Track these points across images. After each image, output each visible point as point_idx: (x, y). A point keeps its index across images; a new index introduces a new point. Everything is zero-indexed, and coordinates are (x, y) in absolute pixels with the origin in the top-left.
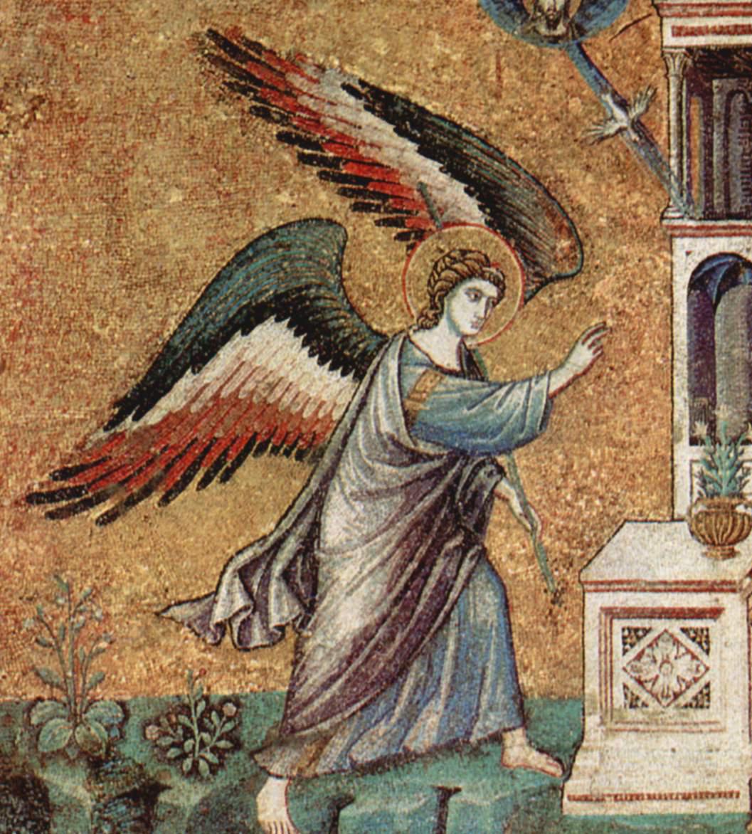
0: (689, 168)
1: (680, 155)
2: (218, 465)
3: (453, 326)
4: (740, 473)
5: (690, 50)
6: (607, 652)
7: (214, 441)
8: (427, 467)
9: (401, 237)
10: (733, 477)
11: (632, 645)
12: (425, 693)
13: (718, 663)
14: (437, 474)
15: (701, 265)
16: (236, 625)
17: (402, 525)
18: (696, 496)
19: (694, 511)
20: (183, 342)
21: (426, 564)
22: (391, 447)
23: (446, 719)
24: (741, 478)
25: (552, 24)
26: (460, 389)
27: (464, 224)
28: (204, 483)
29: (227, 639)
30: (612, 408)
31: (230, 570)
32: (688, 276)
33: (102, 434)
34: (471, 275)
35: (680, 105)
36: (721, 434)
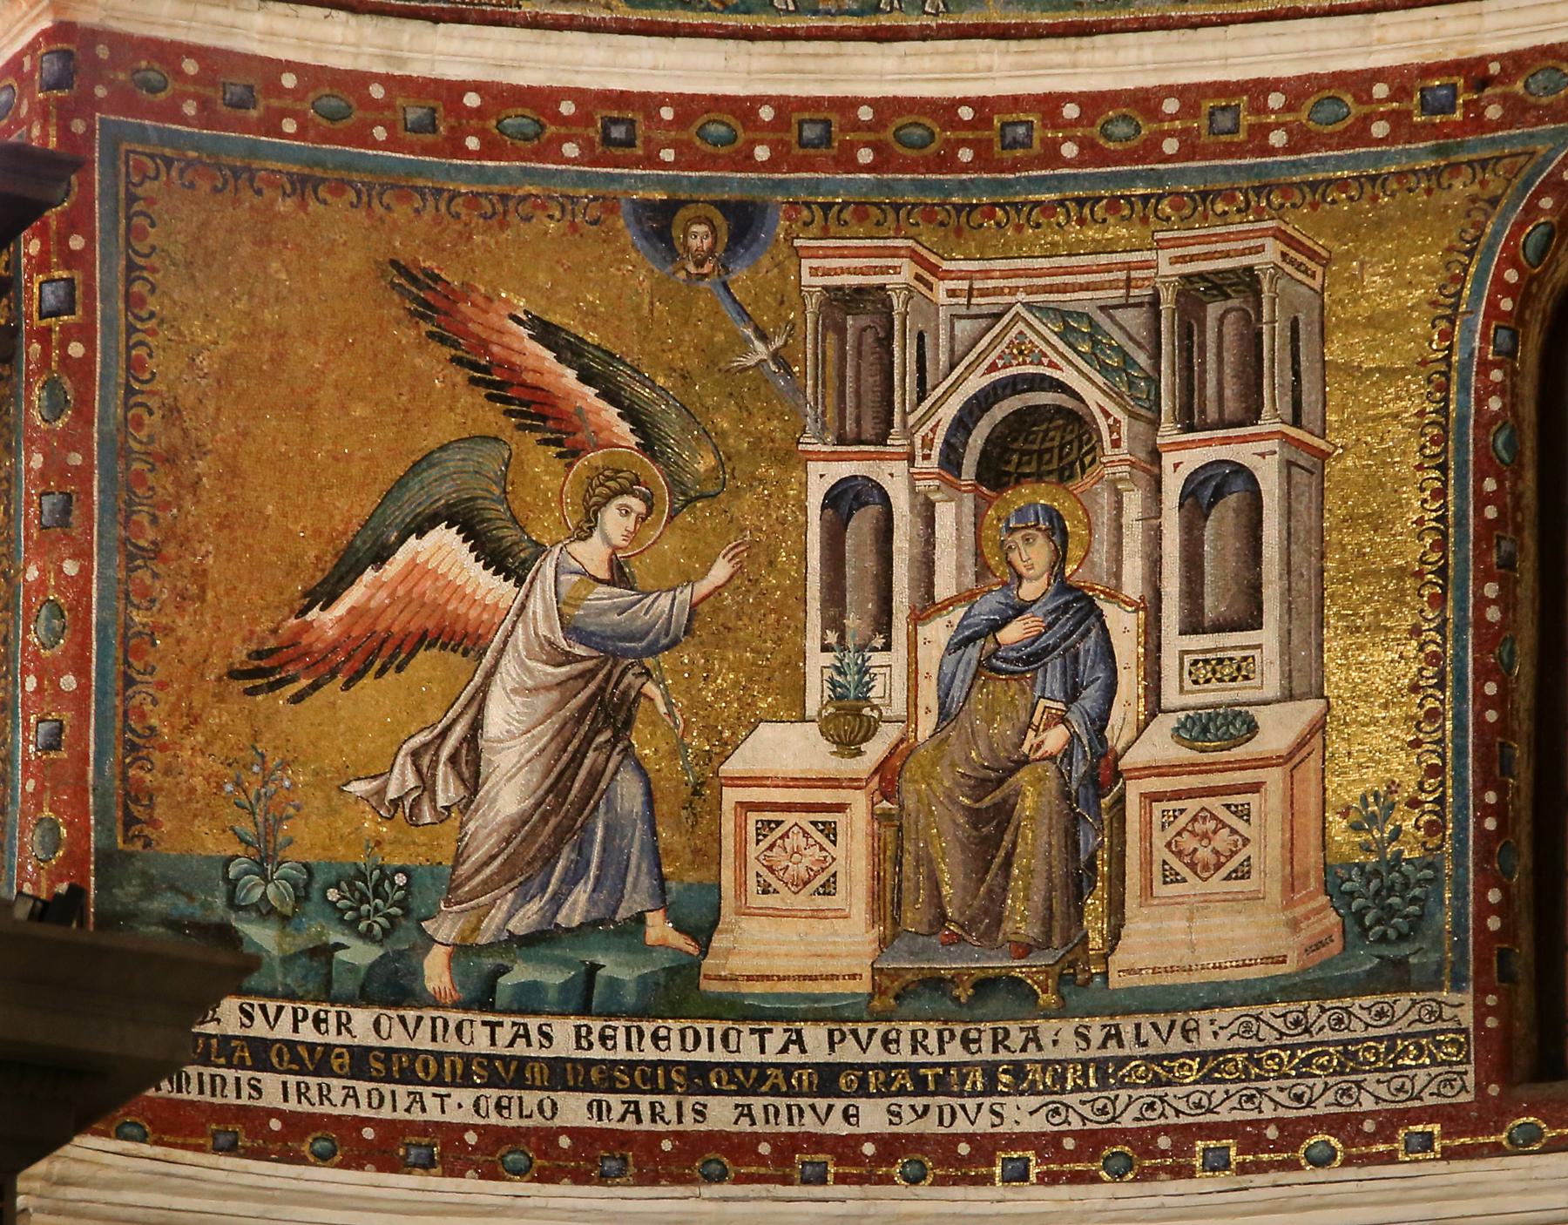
0: (823, 397)
1: (816, 385)
3: (606, 539)
4: (867, 678)
5: (825, 288)
8: (580, 667)
10: (860, 680)
12: (573, 877)
14: (588, 674)
15: (833, 487)
18: (826, 699)
19: (824, 714)
21: (579, 756)
22: (547, 648)
25: (700, 264)
34: (623, 492)
35: (816, 339)
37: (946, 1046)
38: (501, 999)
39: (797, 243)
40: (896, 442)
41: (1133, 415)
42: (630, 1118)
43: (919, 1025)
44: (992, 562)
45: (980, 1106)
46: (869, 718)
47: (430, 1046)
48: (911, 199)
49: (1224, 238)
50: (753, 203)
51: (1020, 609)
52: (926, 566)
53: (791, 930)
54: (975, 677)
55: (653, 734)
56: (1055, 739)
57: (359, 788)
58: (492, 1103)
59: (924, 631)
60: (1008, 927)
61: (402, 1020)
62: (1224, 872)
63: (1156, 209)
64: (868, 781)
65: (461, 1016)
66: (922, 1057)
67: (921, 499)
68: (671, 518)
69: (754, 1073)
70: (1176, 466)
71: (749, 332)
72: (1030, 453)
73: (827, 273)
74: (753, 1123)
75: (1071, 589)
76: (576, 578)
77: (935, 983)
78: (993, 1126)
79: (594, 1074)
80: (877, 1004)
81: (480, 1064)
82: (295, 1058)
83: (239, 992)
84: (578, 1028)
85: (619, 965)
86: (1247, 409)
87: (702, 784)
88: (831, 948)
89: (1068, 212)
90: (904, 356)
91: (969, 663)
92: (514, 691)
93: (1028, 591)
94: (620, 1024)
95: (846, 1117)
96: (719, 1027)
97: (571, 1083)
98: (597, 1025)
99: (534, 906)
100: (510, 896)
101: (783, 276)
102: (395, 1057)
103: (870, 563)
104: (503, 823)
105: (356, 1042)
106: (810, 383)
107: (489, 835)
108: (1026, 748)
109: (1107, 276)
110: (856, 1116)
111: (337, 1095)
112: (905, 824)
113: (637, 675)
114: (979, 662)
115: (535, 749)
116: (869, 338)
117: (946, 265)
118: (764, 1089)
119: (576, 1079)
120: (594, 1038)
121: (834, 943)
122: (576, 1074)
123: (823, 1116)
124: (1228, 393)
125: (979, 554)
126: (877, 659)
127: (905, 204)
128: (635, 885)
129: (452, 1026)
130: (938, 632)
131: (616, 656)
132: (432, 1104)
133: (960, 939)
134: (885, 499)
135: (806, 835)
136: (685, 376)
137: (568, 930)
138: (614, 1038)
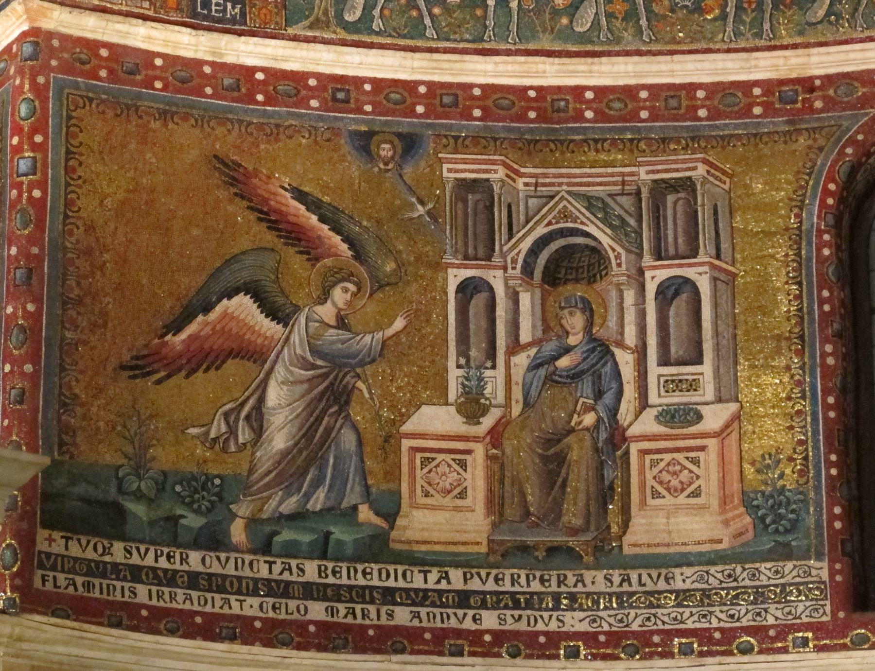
0: (456, 235)
1: (451, 228)
2: (213, 363)
3: (334, 304)
4: (482, 383)
5: (456, 179)
6: (412, 469)
7: (212, 350)
8: (319, 371)
9: (308, 260)
11: (426, 466)
12: (317, 483)
13: (470, 477)
14: (325, 376)
16: (221, 440)
17: (308, 398)
18: (459, 394)
19: (459, 401)
20: (198, 301)
21: (319, 420)
23: (327, 497)
24: (483, 386)
25: (386, 164)
26: (338, 335)
27: (340, 256)
28: (207, 370)
29: (217, 445)
30: (416, 349)
31: (219, 413)
32: (455, 287)
33: (156, 341)
36: (472, 364)
37: (532, 583)
38: (275, 549)
39: (440, 155)
40: (497, 260)
41: (628, 251)
42: (350, 617)
43: (516, 571)
44: (552, 325)
45: (551, 616)
46: (484, 405)
47: (234, 573)
48: (503, 136)
49: (675, 162)
50: (415, 134)
51: (568, 350)
52: (514, 326)
53: (441, 517)
54: (543, 386)
55: (362, 409)
56: (589, 419)
57: (193, 431)
58: (270, 605)
59: (515, 360)
60: (565, 519)
61: (218, 558)
62: (686, 493)
63: (637, 146)
64: (484, 438)
65: (252, 557)
66: (517, 588)
67: (511, 290)
68: (371, 295)
69: (421, 594)
70: (653, 278)
71: (414, 200)
72: (572, 268)
73: (457, 171)
74: (421, 622)
75: (595, 340)
76: (317, 324)
77: (524, 549)
78: (559, 627)
79: (329, 592)
80: (491, 559)
81: (263, 584)
82: (156, 576)
83: (122, 538)
84: (319, 567)
85: (343, 533)
86: (691, 250)
87: (390, 436)
88: (464, 527)
89: (589, 145)
90: (500, 216)
91: (540, 377)
92: (282, 383)
93: (572, 340)
94: (344, 565)
95: (474, 619)
96: (400, 569)
97: (316, 596)
98: (330, 565)
99: (293, 500)
100: (280, 493)
101: (433, 171)
102: (214, 578)
103: (484, 323)
104: (276, 454)
105: (192, 569)
106: (448, 227)
107: (269, 459)
108: (573, 423)
109: (611, 179)
110: (480, 619)
111: (180, 598)
112: (506, 462)
113: (353, 377)
114: (546, 377)
115: (294, 414)
116: (481, 206)
117: (523, 170)
118: (427, 603)
119: (318, 594)
120: (329, 572)
121: (466, 525)
122: (318, 591)
123: (461, 619)
124: (680, 241)
125: (544, 320)
126: (488, 373)
127: (499, 138)
128: (352, 489)
129: (247, 562)
130: (522, 360)
131: (341, 367)
132: (235, 605)
133: (538, 525)
134: (491, 289)
135: (449, 466)
136: (378, 222)
137: (314, 512)
138: (340, 572)
